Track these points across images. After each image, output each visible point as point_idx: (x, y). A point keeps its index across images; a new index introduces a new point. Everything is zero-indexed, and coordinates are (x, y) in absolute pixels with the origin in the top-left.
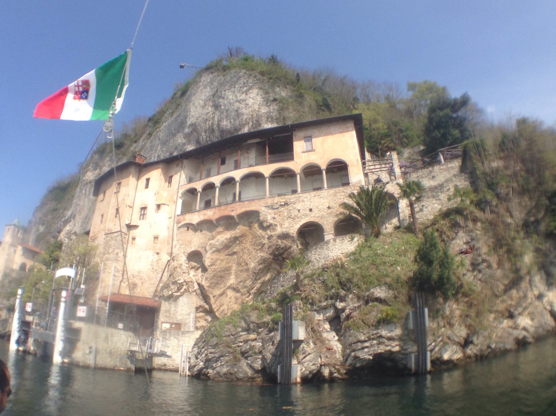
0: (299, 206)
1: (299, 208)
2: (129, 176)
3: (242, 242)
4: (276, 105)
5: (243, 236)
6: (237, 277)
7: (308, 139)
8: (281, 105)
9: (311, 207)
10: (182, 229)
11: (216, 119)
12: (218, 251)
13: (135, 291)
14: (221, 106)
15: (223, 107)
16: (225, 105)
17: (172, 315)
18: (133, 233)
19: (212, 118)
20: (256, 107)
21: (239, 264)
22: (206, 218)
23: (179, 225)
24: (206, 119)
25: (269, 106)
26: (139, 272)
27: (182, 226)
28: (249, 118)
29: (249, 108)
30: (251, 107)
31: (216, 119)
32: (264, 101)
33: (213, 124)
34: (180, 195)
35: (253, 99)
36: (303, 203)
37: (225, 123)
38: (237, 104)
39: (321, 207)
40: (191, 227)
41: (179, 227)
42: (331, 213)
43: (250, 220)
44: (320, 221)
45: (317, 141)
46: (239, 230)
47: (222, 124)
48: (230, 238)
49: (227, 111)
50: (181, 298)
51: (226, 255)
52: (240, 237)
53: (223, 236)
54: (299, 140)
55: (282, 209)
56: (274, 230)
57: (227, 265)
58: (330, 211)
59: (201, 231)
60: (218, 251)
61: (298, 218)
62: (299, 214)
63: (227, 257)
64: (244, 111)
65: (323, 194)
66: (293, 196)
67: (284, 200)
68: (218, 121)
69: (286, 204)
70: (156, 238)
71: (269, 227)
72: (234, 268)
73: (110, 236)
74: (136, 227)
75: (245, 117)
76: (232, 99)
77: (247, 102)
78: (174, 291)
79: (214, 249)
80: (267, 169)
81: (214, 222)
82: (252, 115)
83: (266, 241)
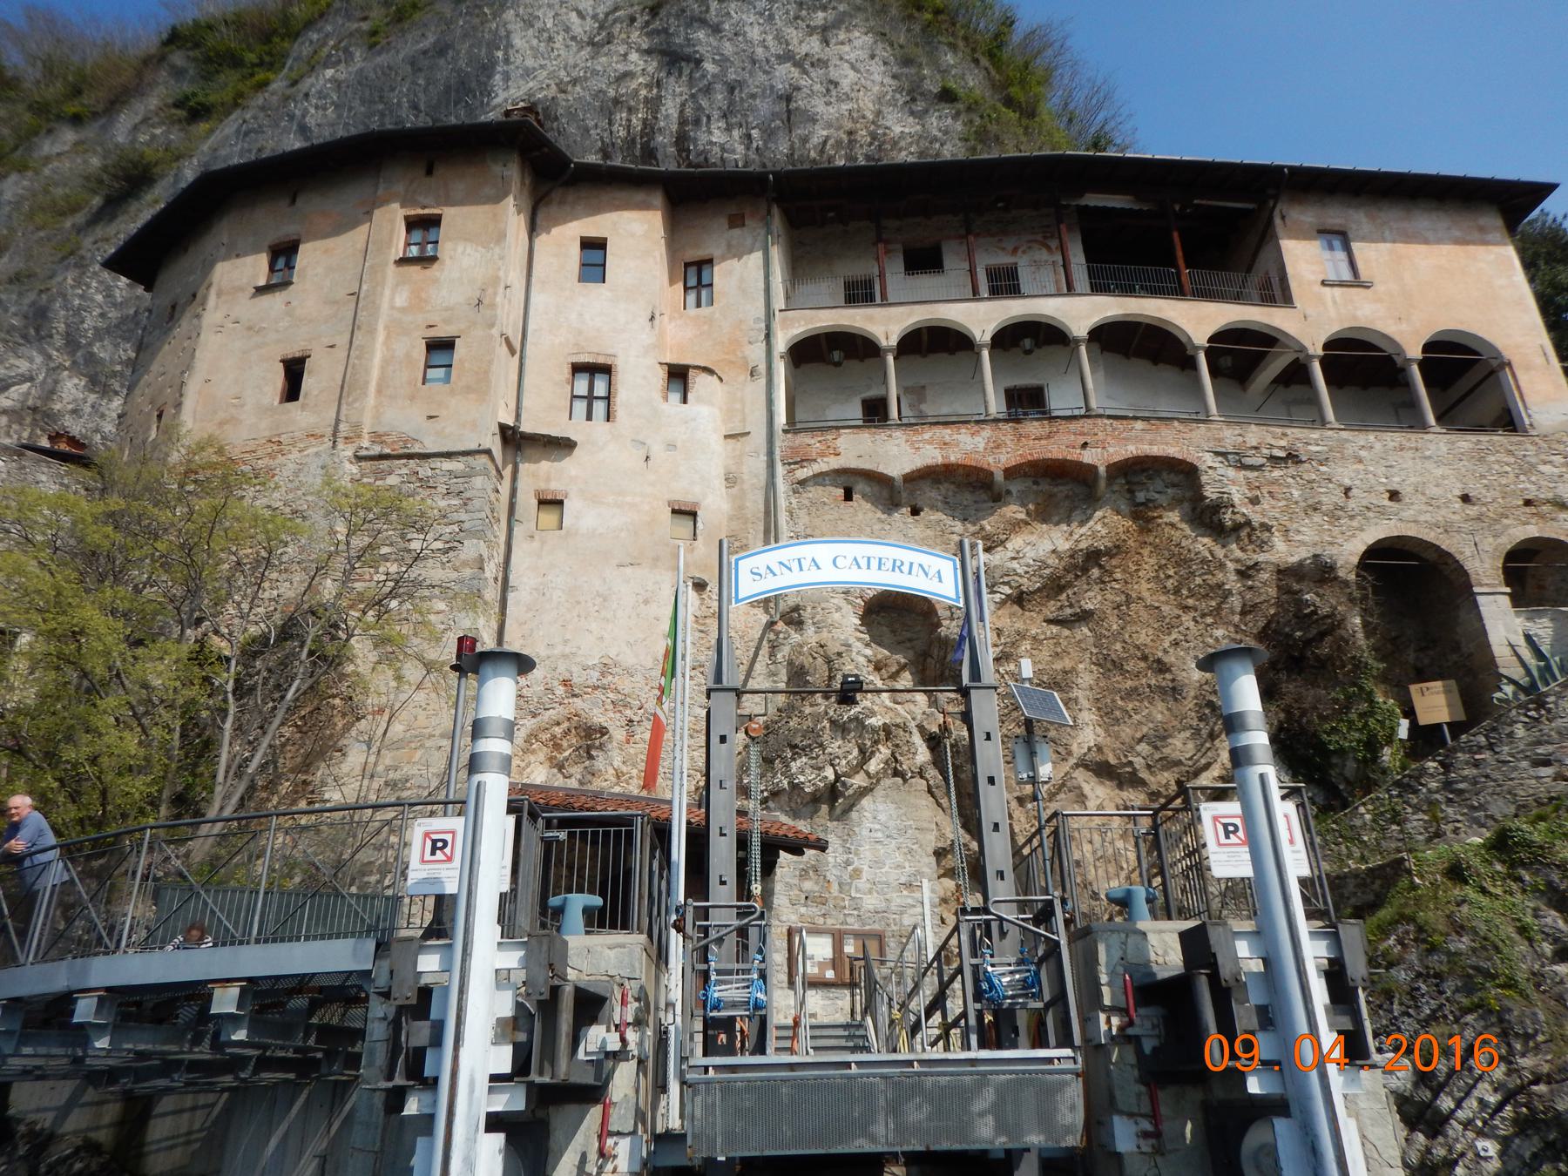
0: (1345, 474)
1: (1347, 482)
2: (498, 199)
3: (1111, 574)
4: (956, 117)
5: (1116, 550)
6: (1109, 716)
7: (1341, 237)
8: (978, 121)
9: (1395, 487)
10: (815, 492)
11: (670, 108)
12: (1020, 599)
13: (600, 763)
14: (698, 62)
15: (709, 67)
16: (723, 62)
17: (835, 887)
18: (538, 474)
19: (647, 100)
20: (867, 105)
21: (1109, 665)
22: (954, 457)
23: (803, 473)
24: (616, 101)
25: (920, 116)
26: (605, 669)
27: (819, 479)
28: (839, 143)
29: (839, 100)
30: (849, 98)
31: (670, 108)
32: (899, 90)
33: (649, 129)
34: (781, 344)
35: (853, 67)
36: (1361, 467)
37: (718, 136)
38: (785, 71)
39: (1433, 491)
40: (860, 486)
41: (802, 483)
42: (1479, 519)
43: (1141, 496)
44: (1445, 544)
45: (1372, 255)
46: (1103, 525)
47: (703, 138)
48: (1073, 554)
49: (731, 90)
50: (866, 802)
51: (1049, 622)
52: (1109, 553)
53: (1041, 545)
54: (1301, 234)
55: (1277, 473)
56: (1262, 545)
57: (1058, 666)
58: (1472, 511)
59: (915, 512)
60: (1020, 599)
61: (1352, 517)
62: (1352, 504)
63: (1055, 629)
64: (819, 106)
65: (1433, 447)
66: (1315, 435)
67: (1283, 443)
68: (683, 122)
69: (1292, 458)
70: (685, 513)
71: (1240, 531)
72: (1086, 677)
73: (403, 468)
74: (561, 446)
75: (820, 133)
76: (763, 43)
77: (834, 74)
78: (843, 766)
79: (1007, 590)
80: (1197, 320)
81: (999, 477)
82: (850, 133)
83: (1232, 582)
